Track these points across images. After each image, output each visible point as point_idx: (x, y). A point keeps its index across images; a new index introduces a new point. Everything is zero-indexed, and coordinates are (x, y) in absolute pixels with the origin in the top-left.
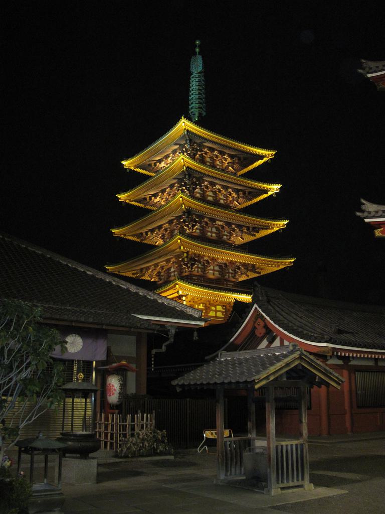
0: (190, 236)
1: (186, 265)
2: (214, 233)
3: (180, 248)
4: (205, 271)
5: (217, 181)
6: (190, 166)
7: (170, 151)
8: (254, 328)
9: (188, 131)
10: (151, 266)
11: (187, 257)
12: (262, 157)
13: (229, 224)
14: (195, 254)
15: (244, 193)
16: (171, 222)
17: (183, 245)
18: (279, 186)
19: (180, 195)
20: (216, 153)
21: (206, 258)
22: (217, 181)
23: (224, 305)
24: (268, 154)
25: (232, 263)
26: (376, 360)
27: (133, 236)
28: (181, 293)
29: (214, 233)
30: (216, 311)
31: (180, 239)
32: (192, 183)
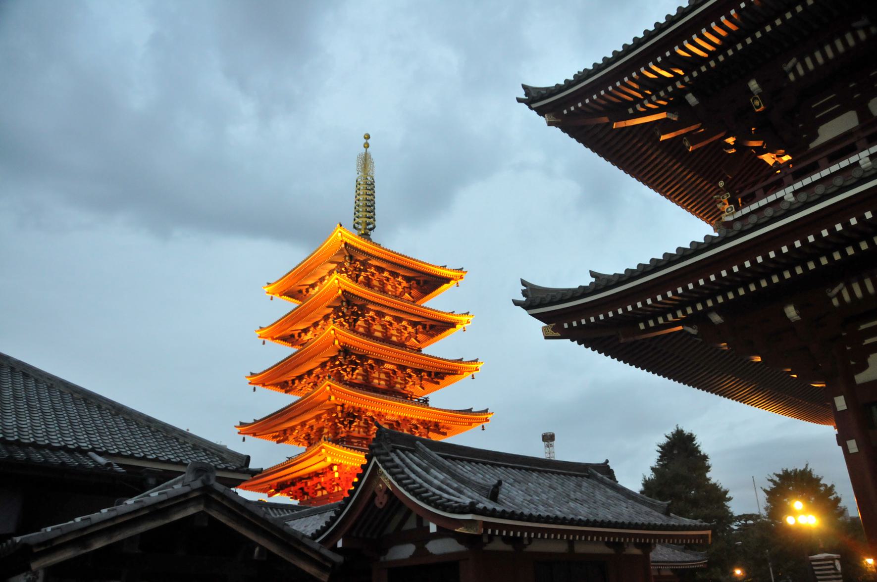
0: (351, 385)
1: (342, 423)
3: (329, 399)
4: (369, 431)
5: (385, 311)
6: (348, 289)
9: (346, 244)
10: (296, 426)
11: (342, 412)
13: (403, 368)
14: (353, 407)
15: (424, 327)
16: (323, 365)
17: (333, 394)
19: (332, 327)
20: (386, 274)
21: (369, 414)
22: (385, 311)
25: (406, 420)
31: (329, 385)
32: (353, 313)
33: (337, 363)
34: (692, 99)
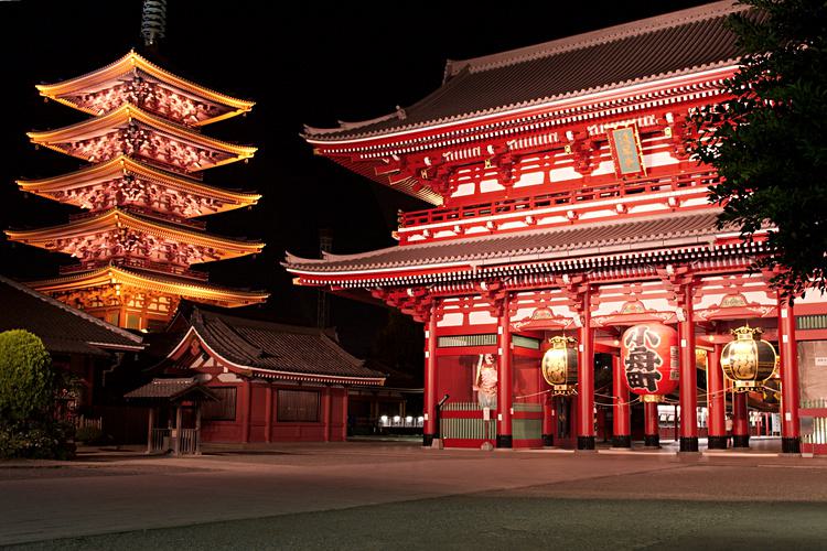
0: (130, 209)
1: (123, 243)
7: (110, 85)
8: (190, 347)
9: (138, 69)
12: (235, 109)
15: (207, 154)
16: (106, 184)
18: (254, 150)
20: (174, 96)
21: (150, 237)
23: (168, 296)
24: (243, 106)
26: (300, 382)
27: (50, 193)
28: (114, 281)
30: (158, 304)
33: (121, 185)
34: (396, 158)
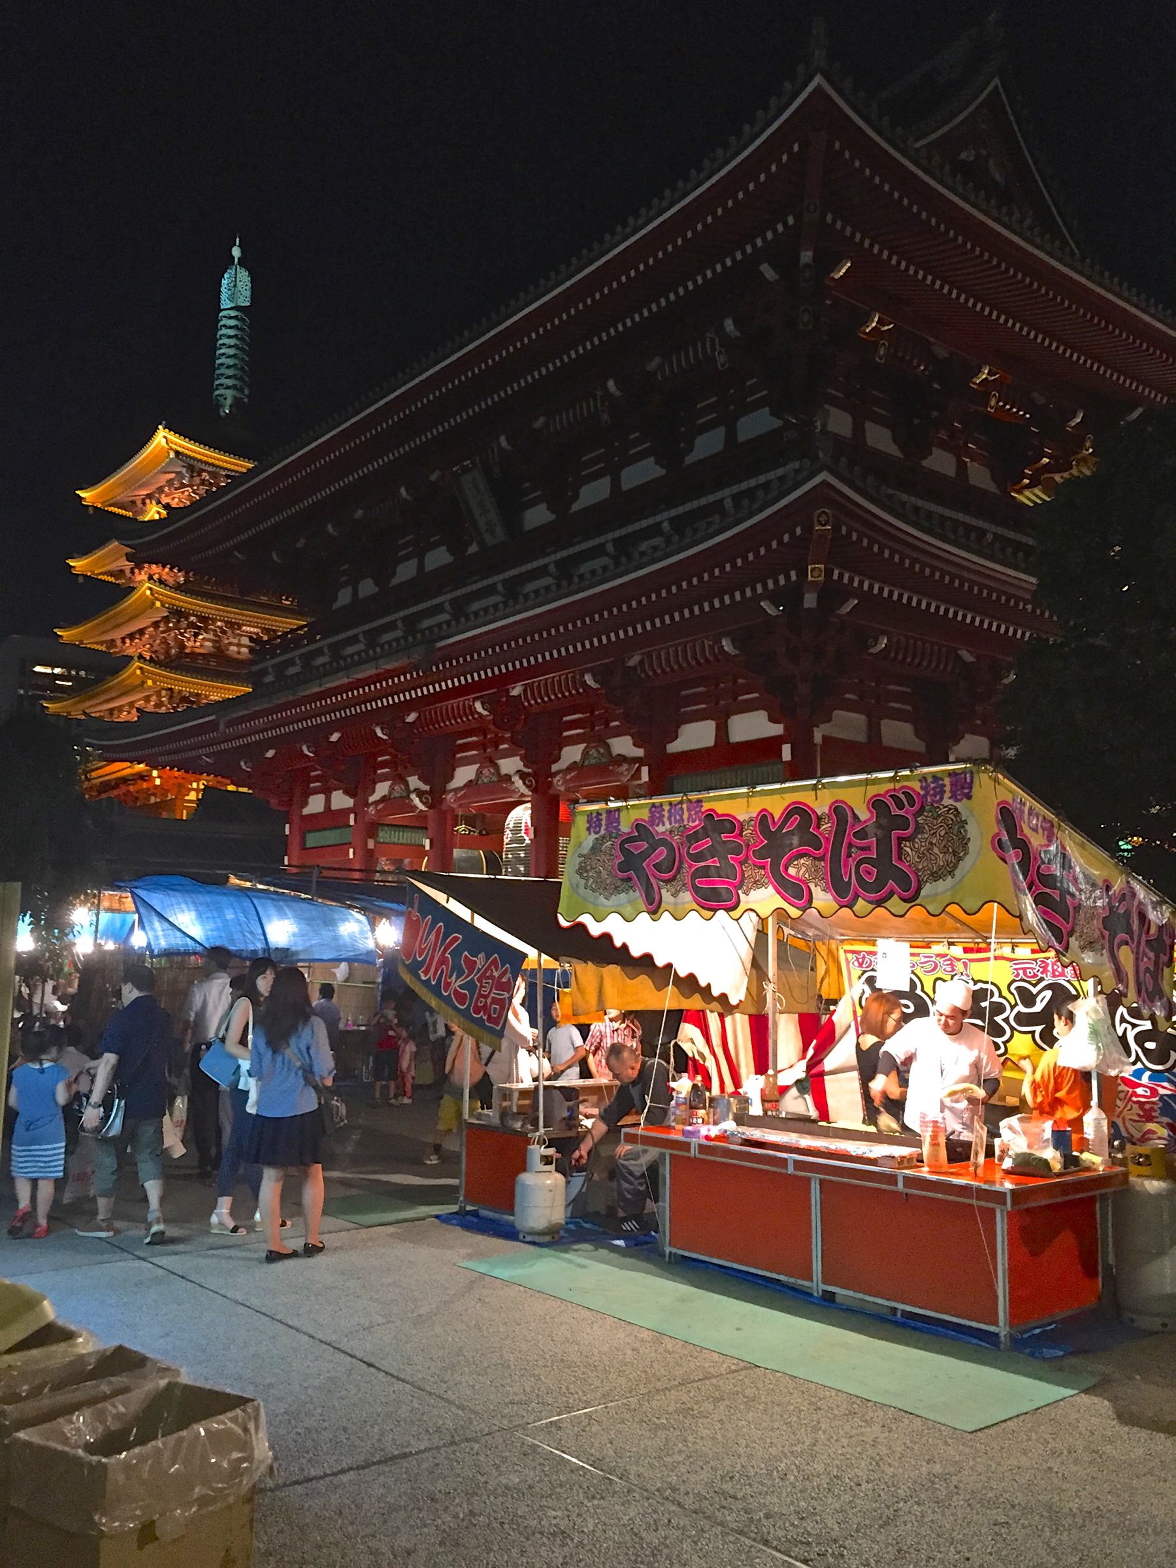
2: (245, 646)
9: (177, 453)
11: (171, 697)
29: (245, 646)
